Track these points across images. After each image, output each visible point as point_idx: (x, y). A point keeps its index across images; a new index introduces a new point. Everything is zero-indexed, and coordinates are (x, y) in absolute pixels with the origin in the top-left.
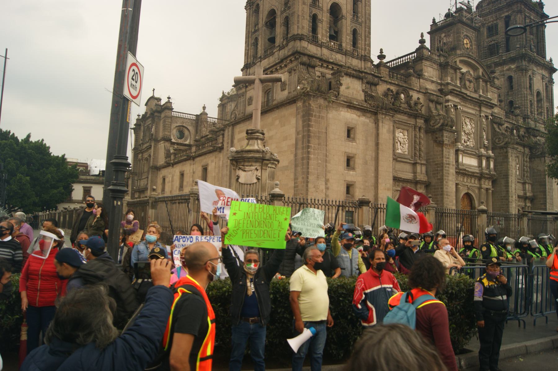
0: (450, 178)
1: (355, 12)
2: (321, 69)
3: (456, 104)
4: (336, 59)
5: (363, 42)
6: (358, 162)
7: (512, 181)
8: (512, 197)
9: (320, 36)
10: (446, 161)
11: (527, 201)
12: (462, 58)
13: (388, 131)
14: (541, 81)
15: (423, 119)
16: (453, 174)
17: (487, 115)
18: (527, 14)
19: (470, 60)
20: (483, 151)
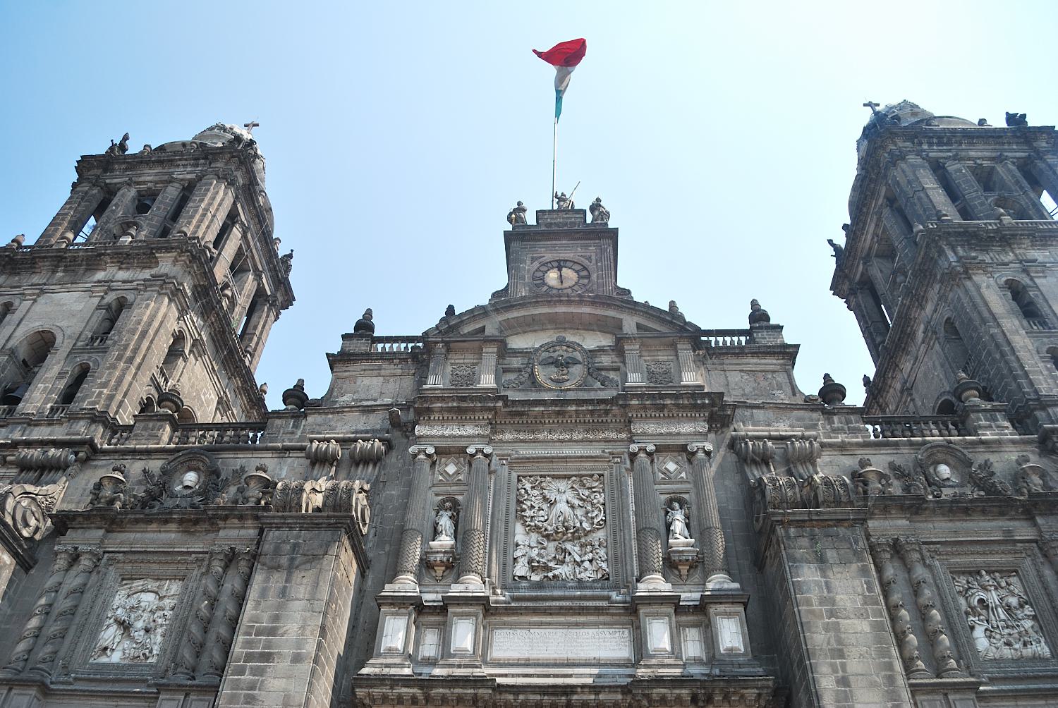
3: (463, 444)
7: (844, 681)
10: (248, 644)
15: (249, 522)
17: (681, 441)
18: (931, 155)
20: (656, 584)
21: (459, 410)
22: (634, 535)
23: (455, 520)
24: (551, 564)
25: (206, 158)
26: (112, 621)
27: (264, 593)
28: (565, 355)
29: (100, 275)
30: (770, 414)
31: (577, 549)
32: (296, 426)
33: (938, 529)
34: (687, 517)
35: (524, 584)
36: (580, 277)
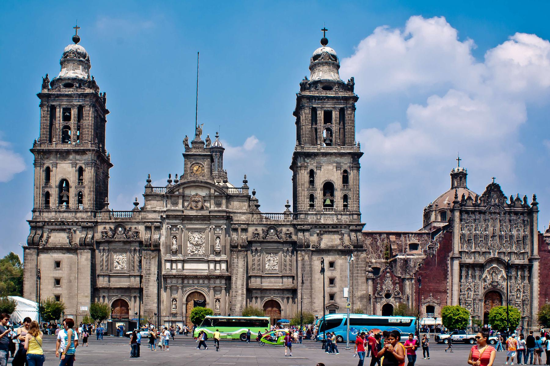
0: (151, 284)
1: (80, 180)
2: (48, 227)
4: (63, 216)
5: (87, 199)
6: (63, 282)
7: (237, 279)
8: (236, 292)
9: (51, 205)
10: (146, 272)
11: (285, 292)
12: (185, 186)
13: (86, 260)
14: (335, 170)
16: (154, 281)
19: (197, 184)
20: (212, 257)
21: (175, 217)
22: (209, 246)
23: (176, 241)
24: (194, 251)
25: (83, 95)
26: (115, 261)
27: (146, 263)
28: (198, 199)
29: (71, 157)
30: (241, 215)
31: (199, 247)
32: (139, 214)
33: (266, 246)
34: (220, 241)
35: (190, 255)
36: (202, 170)
